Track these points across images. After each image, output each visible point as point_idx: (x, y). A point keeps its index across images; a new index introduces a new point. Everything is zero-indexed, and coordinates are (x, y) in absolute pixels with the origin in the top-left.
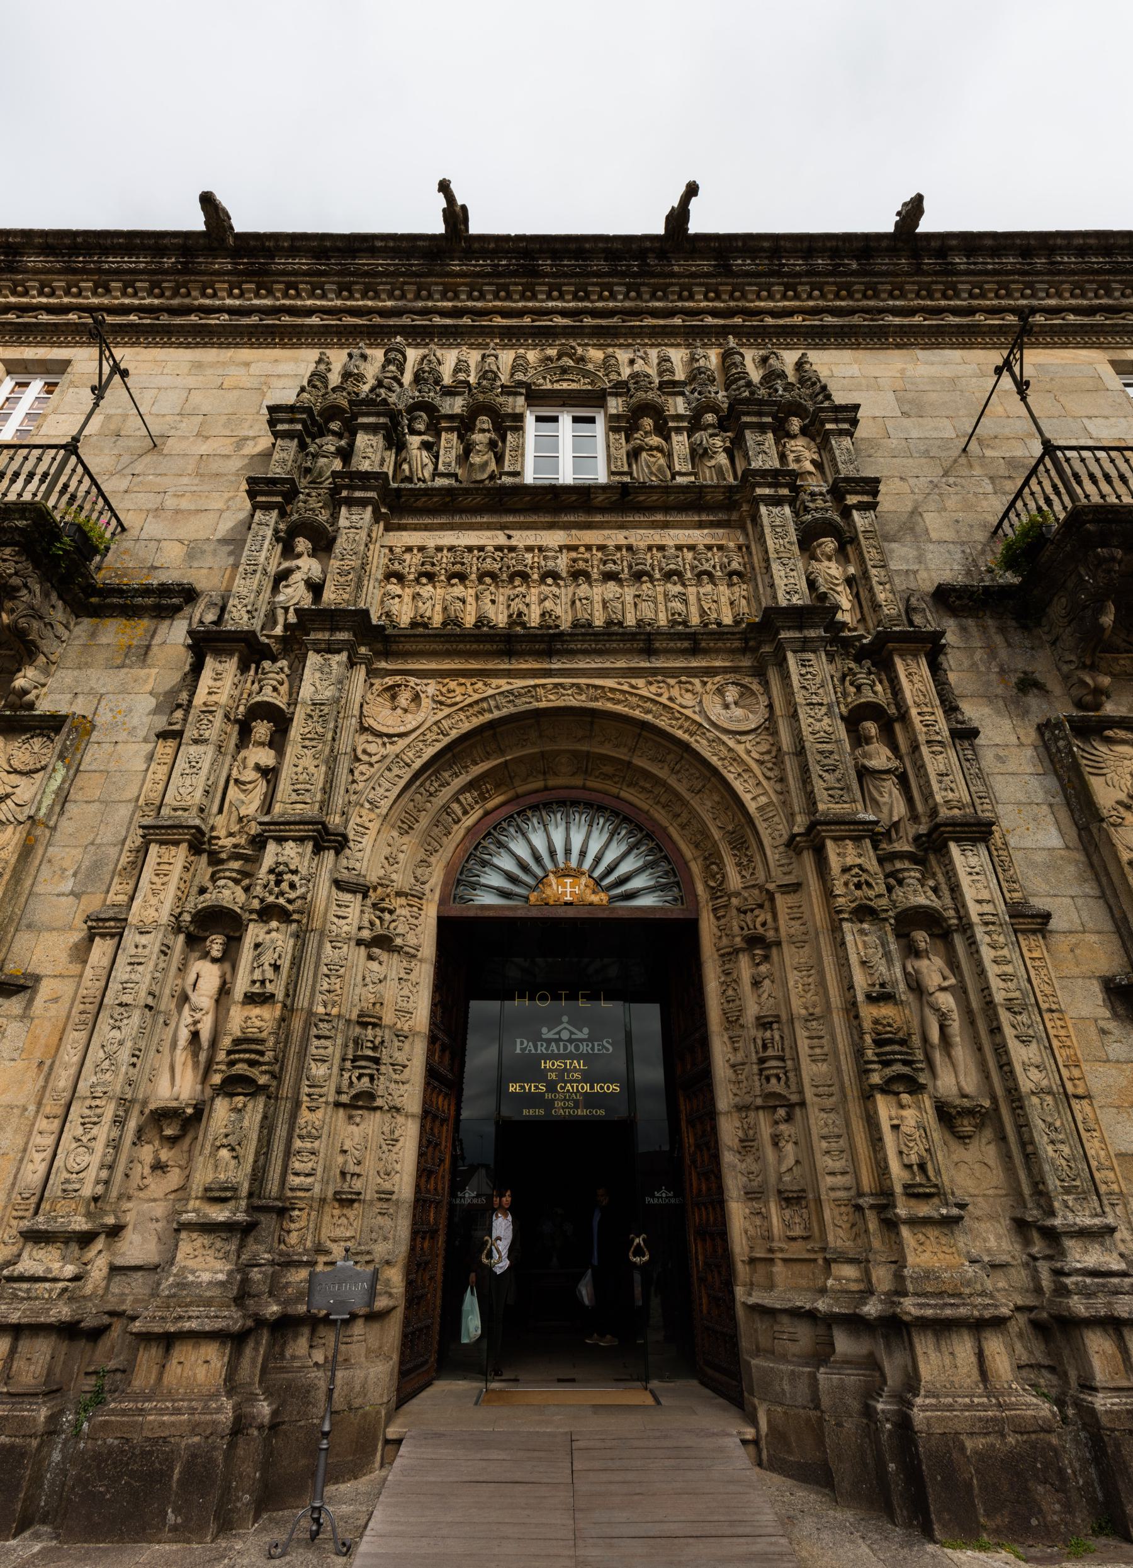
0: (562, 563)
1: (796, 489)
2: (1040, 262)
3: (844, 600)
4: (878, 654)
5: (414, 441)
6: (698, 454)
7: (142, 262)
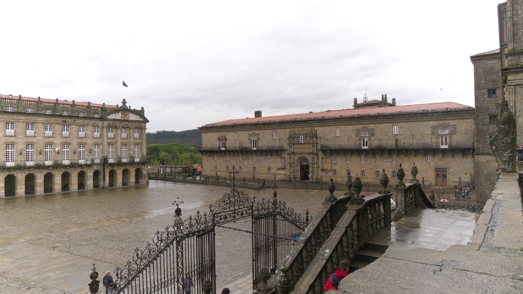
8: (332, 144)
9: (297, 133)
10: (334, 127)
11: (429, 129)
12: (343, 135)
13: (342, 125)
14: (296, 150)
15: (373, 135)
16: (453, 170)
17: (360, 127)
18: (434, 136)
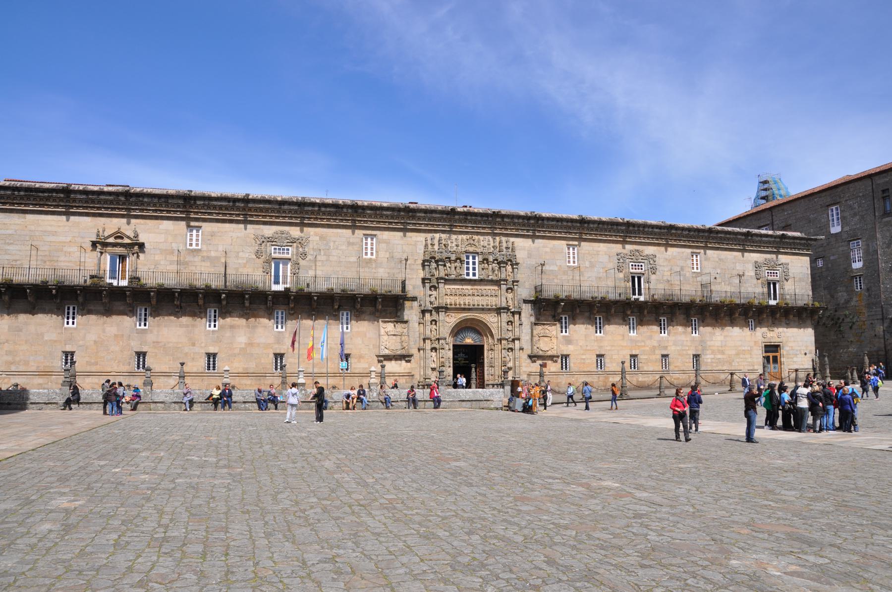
0: (471, 293)
3: (510, 302)
4: (513, 313)
5: (448, 265)
8: (560, 284)
9: (452, 246)
12: (587, 264)
14: (449, 300)
15: (654, 270)
18: (759, 281)
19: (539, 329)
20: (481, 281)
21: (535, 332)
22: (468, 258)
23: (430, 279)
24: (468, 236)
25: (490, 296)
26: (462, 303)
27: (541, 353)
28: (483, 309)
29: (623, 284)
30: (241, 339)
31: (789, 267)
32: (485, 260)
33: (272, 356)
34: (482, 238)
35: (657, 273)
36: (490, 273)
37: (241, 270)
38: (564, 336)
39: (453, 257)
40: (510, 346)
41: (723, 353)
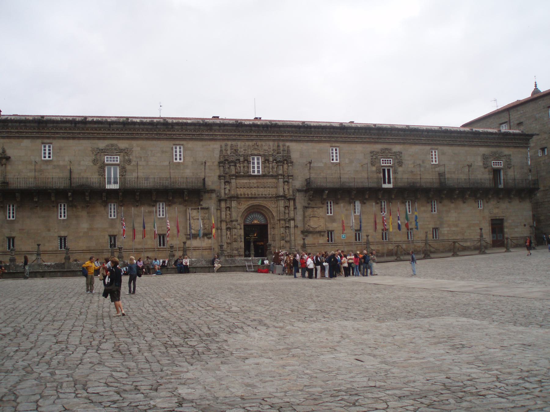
1: (284, 176)
2: (324, 130)
3: (287, 191)
4: (289, 200)
5: (238, 165)
6: (273, 168)
7: (192, 127)
9: (241, 151)
10: (328, 145)
11: (479, 158)
12: (347, 161)
13: (345, 142)
14: (240, 191)
15: (400, 163)
16: (510, 221)
17: (378, 147)
18: (487, 170)
19: (309, 212)
20: (264, 176)
21: (307, 214)
22: (253, 159)
23: (224, 177)
24: (254, 142)
25: (269, 188)
26: (249, 193)
27: (311, 229)
28: (265, 198)
29: (375, 175)
30: (85, 225)
31: (512, 158)
32: (266, 161)
33: (107, 238)
34: (264, 144)
35: (403, 166)
36: (271, 170)
37: (82, 174)
38: (329, 216)
39: (242, 159)
40: (287, 225)
41: (456, 226)
